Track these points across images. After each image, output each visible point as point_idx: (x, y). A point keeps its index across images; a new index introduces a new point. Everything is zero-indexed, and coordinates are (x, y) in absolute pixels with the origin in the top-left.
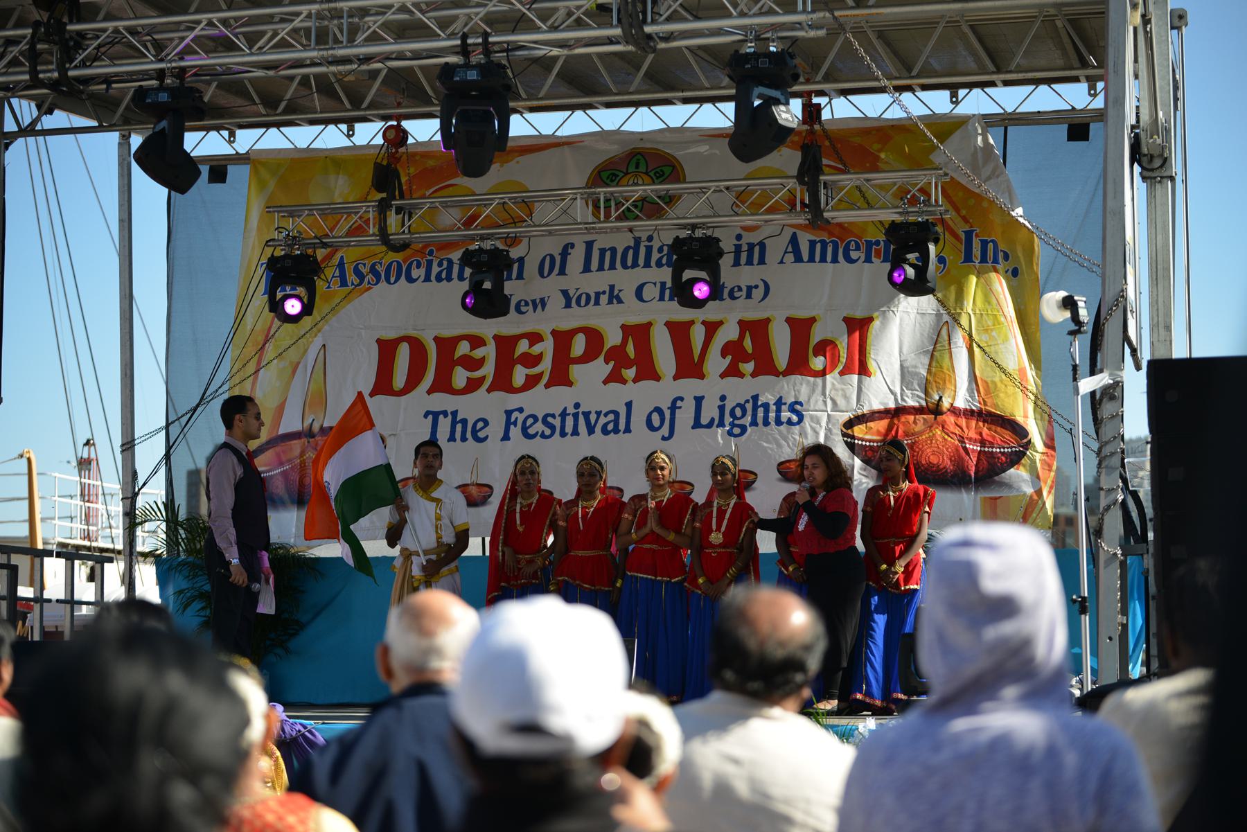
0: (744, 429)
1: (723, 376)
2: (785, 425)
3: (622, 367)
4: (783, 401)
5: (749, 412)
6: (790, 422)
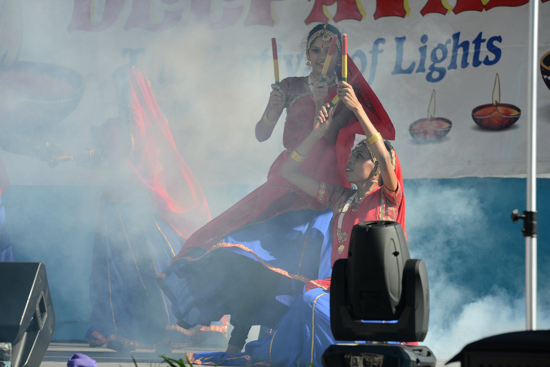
0: (442, 73)
1: (424, 11)
2: (482, 64)
3: (323, 3)
4: (483, 38)
5: (450, 54)
6: (487, 62)
